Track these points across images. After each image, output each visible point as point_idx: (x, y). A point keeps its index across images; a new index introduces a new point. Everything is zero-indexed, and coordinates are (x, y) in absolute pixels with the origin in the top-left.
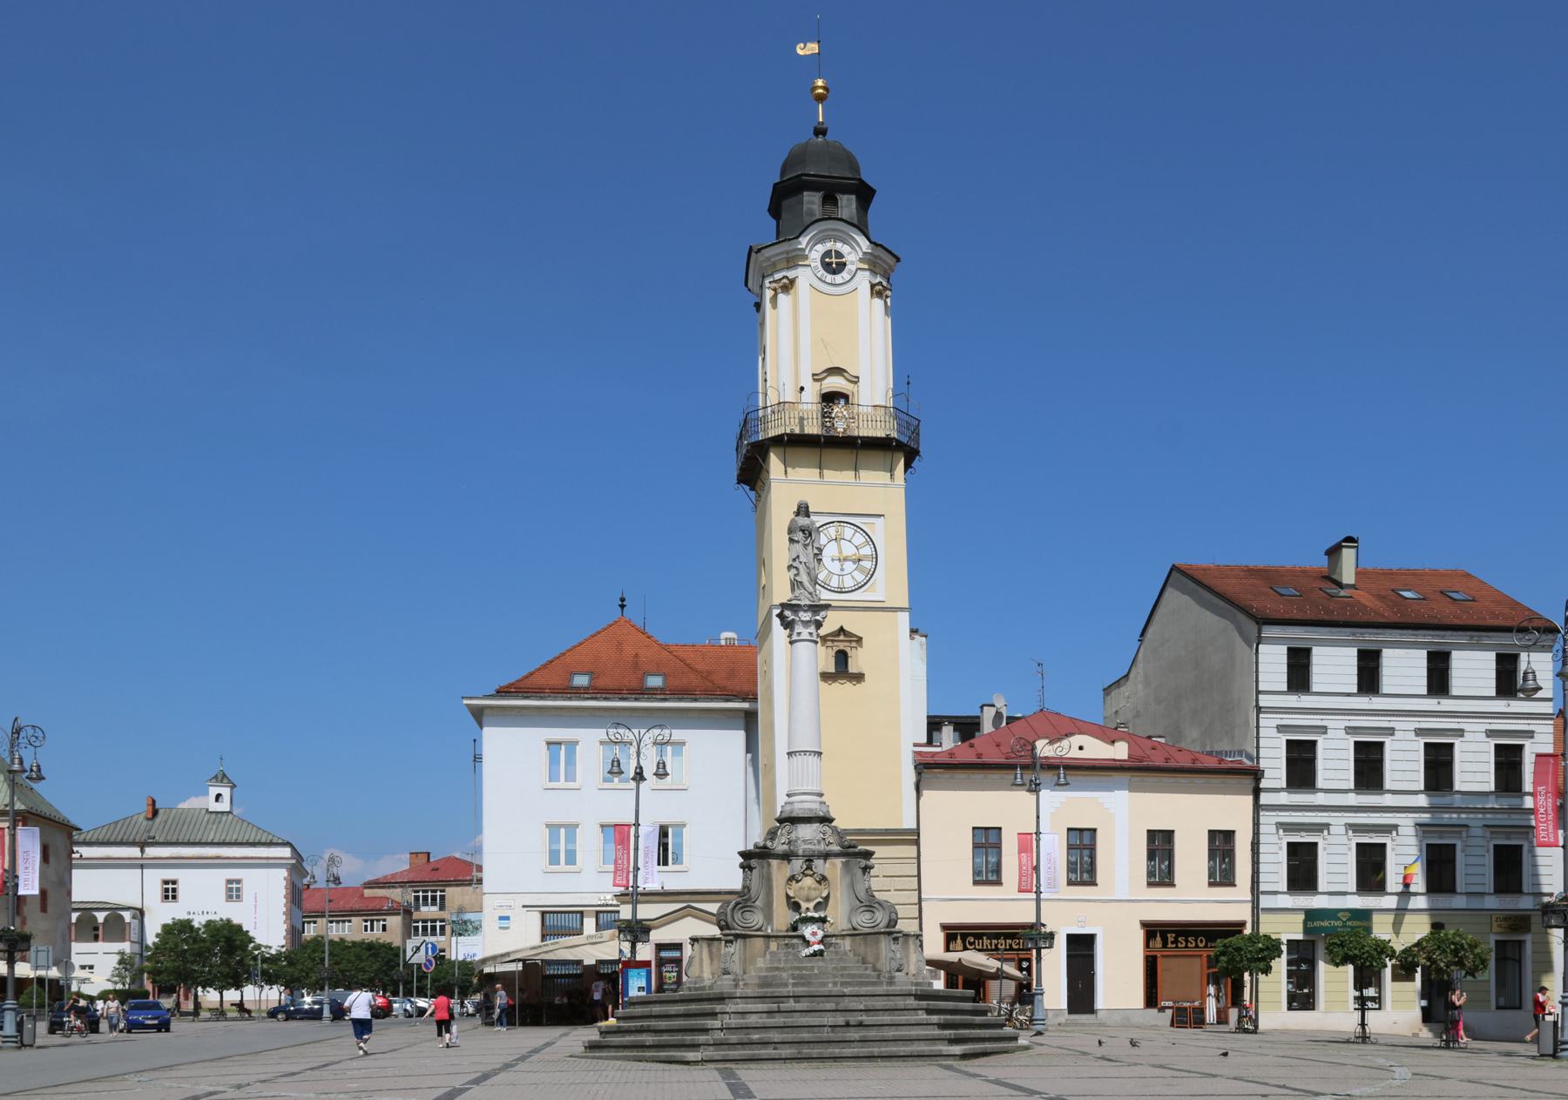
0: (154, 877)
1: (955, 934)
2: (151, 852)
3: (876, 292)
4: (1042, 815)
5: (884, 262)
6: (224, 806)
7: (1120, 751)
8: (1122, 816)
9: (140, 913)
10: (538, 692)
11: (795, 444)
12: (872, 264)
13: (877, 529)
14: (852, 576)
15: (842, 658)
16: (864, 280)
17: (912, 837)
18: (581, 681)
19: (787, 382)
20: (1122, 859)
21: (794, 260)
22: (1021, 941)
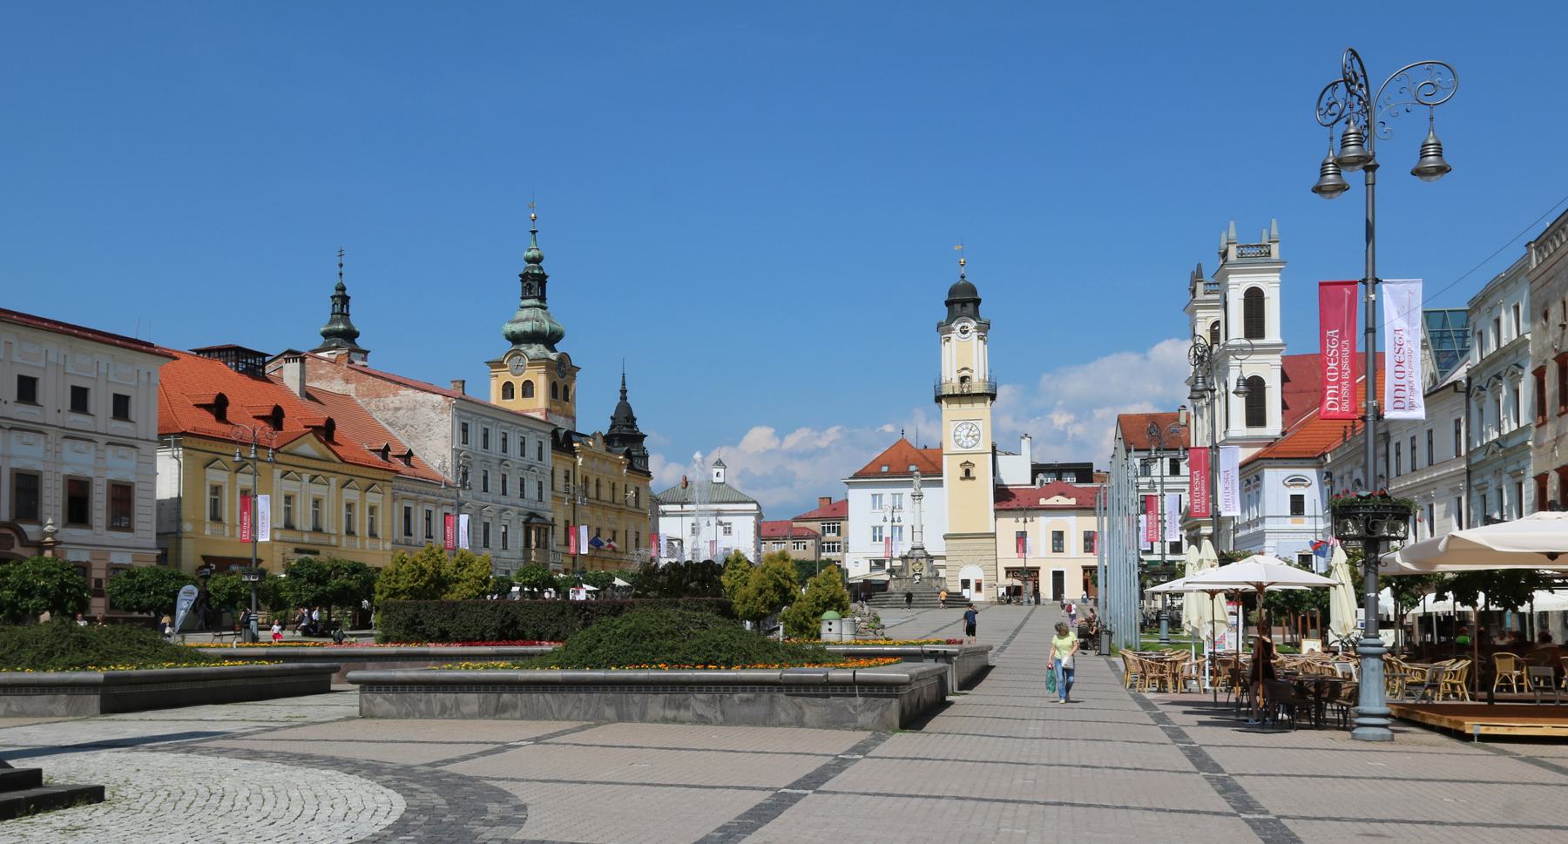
0: (688, 521)
1: (1010, 571)
2: (686, 507)
3: (980, 338)
4: (1040, 528)
5: (984, 328)
6: (721, 480)
7: (1073, 502)
8: (1075, 527)
9: (681, 542)
10: (867, 476)
11: (952, 398)
12: (978, 329)
13: (980, 425)
14: (970, 442)
15: (967, 472)
16: (975, 335)
17: (994, 536)
18: (885, 469)
19: (950, 377)
20: (1074, 542)
21: (950, 331)
22: (1033, 573)
